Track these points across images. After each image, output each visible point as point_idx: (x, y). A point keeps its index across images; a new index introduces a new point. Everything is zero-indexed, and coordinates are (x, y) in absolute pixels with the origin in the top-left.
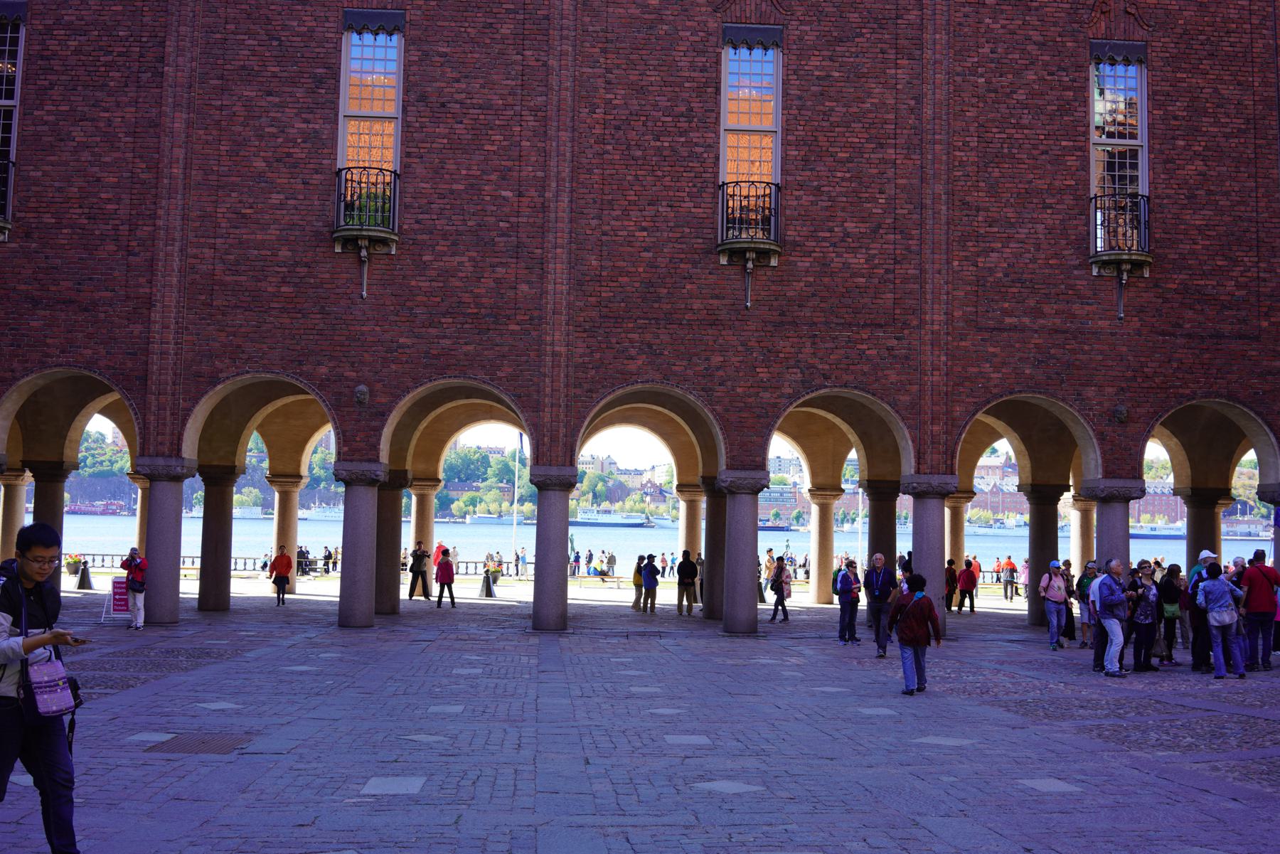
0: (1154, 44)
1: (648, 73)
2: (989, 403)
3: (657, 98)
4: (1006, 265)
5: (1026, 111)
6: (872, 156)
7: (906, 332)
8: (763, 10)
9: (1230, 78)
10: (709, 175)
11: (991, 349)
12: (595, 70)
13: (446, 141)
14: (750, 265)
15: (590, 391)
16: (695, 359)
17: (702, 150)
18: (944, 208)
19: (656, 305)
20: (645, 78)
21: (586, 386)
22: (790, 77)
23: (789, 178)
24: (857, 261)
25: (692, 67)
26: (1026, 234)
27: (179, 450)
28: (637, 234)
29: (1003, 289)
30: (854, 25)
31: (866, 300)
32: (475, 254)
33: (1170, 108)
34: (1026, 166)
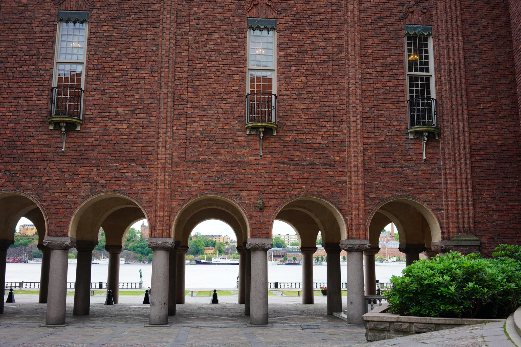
0: (280, 20)
1: (18, 35)
2: (190, 199)
3: (22, 47)
4: (201, 129)
6: (133, 75)
7: (147, 163)
8: (80, 4)
9: (320, 36)
10: (46, 84)
11: (193, 172)
14: (63, 129)
16: (33, 179)
17: (43, 72)
18: (169, 100)
19: (15, 151)
20: (17, 37)
22: (92, 36)
23: (88, 86)
24: (122, 127)
25: (41, 31)
26: (212, 113)
28: (7, 114)
29: (200, 142)
30: (126, 11)
31: (127, 147)
33: (288, 51)
34: (213, 80)
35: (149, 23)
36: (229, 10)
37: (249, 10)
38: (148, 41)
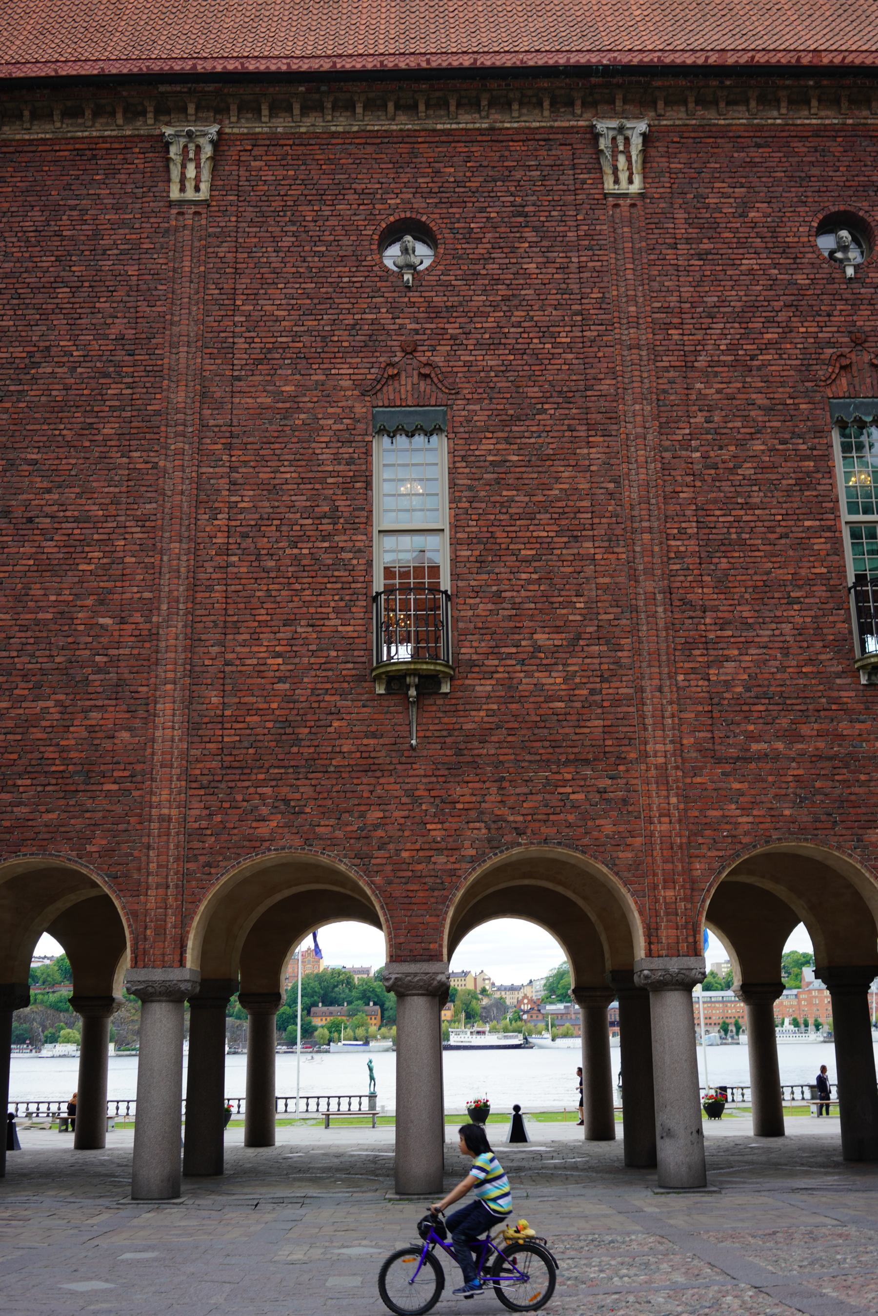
1: (282, 469)
2: (738, 856)
3: (294, 498)
4: (746, 677)
5: (756, 488)
6: (564, 551)
7: (622, 768)
8: (422, 389)
10: (359, 585)
11: (736, 786)
12: (217, 470)
13: (31, 562)
14: (413, 692)
15: (208, 865)
16: (346, 817)
17: (350, 555)
18: (660, 609)
19: (295, 749)
20: (278, 475)
21: (202, 859)
22: (458, 465)
23: (460, 584)
24: (551, 681)
25: (337, 459)
26: (770, 636)
28: (270, 661)
29: (745, 708)
30: (533, 401)
31: (567, 730)
32: (62, 697)
34: (762, 554)
35: (591, 427)
36: (783, 384)
37: (830, 381)
38: (592, 468)
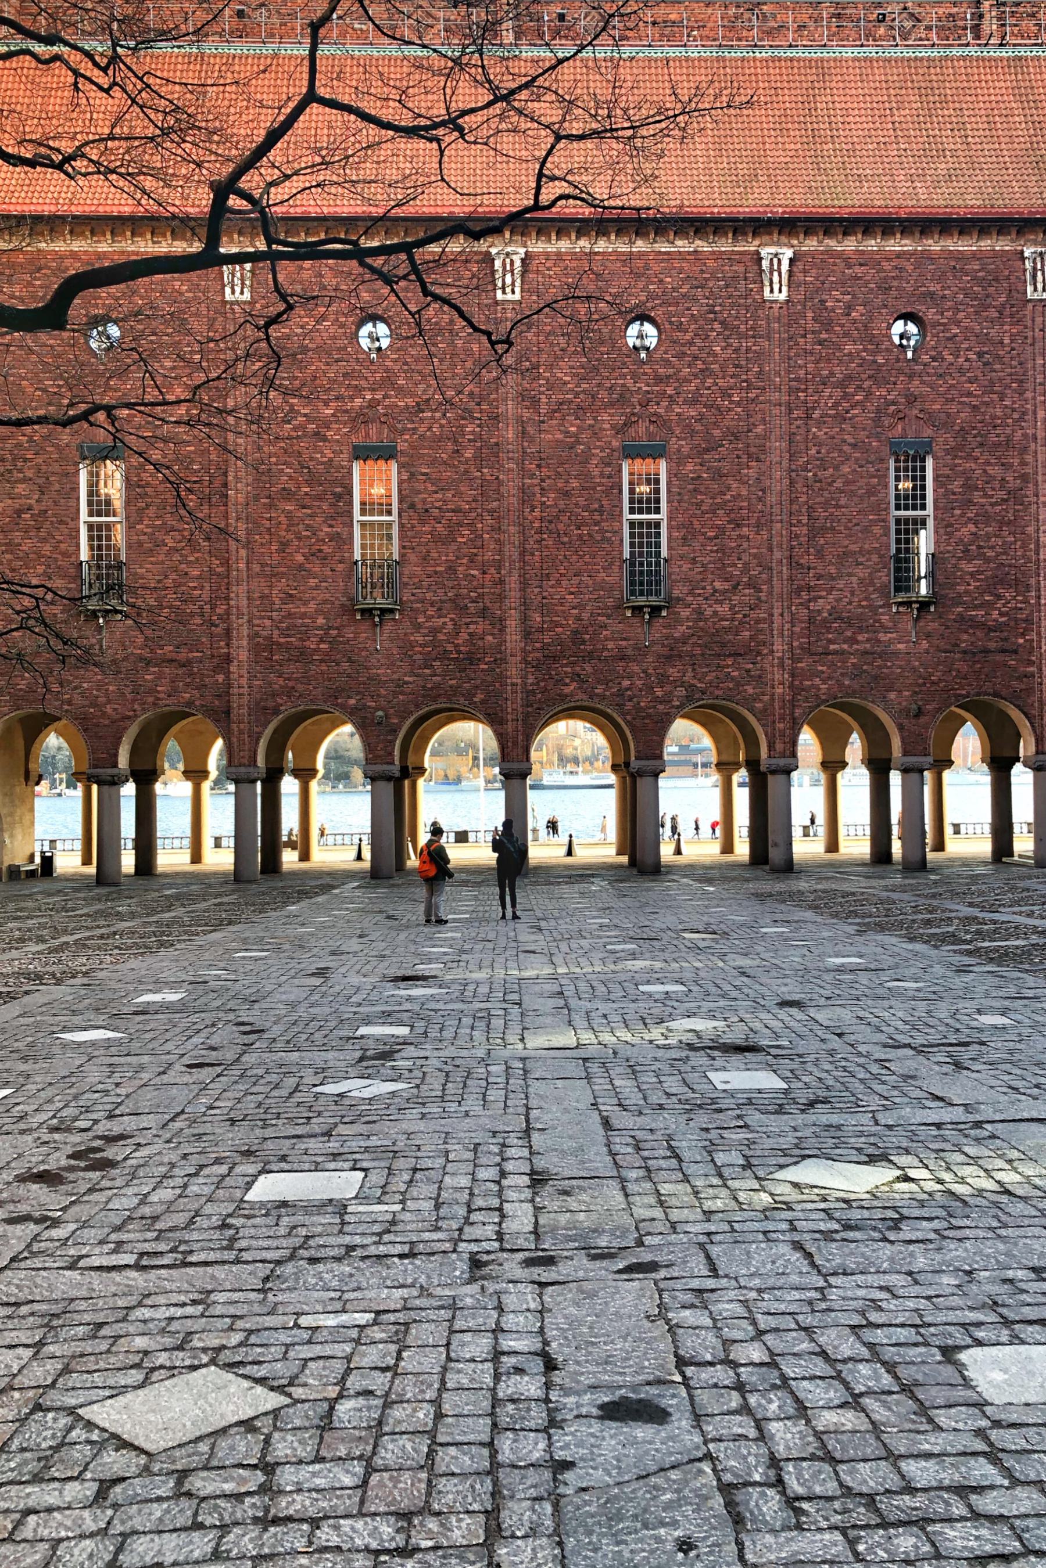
14: (647, 616)
21: (535, 706)
25: (602, 475)
27: (255, 761)
35: (750, 456)
36: (864, 429)
37: (892, 427)
